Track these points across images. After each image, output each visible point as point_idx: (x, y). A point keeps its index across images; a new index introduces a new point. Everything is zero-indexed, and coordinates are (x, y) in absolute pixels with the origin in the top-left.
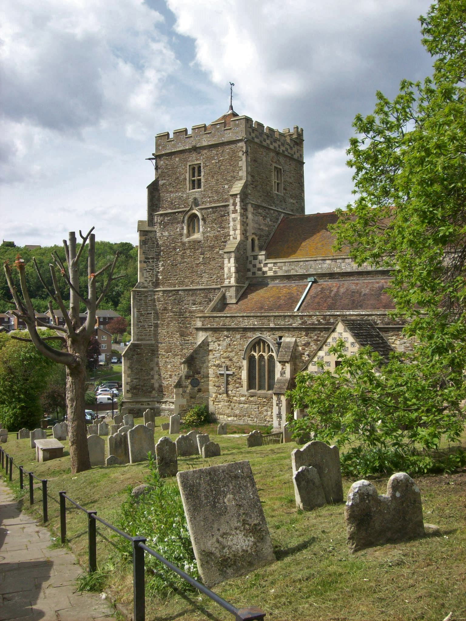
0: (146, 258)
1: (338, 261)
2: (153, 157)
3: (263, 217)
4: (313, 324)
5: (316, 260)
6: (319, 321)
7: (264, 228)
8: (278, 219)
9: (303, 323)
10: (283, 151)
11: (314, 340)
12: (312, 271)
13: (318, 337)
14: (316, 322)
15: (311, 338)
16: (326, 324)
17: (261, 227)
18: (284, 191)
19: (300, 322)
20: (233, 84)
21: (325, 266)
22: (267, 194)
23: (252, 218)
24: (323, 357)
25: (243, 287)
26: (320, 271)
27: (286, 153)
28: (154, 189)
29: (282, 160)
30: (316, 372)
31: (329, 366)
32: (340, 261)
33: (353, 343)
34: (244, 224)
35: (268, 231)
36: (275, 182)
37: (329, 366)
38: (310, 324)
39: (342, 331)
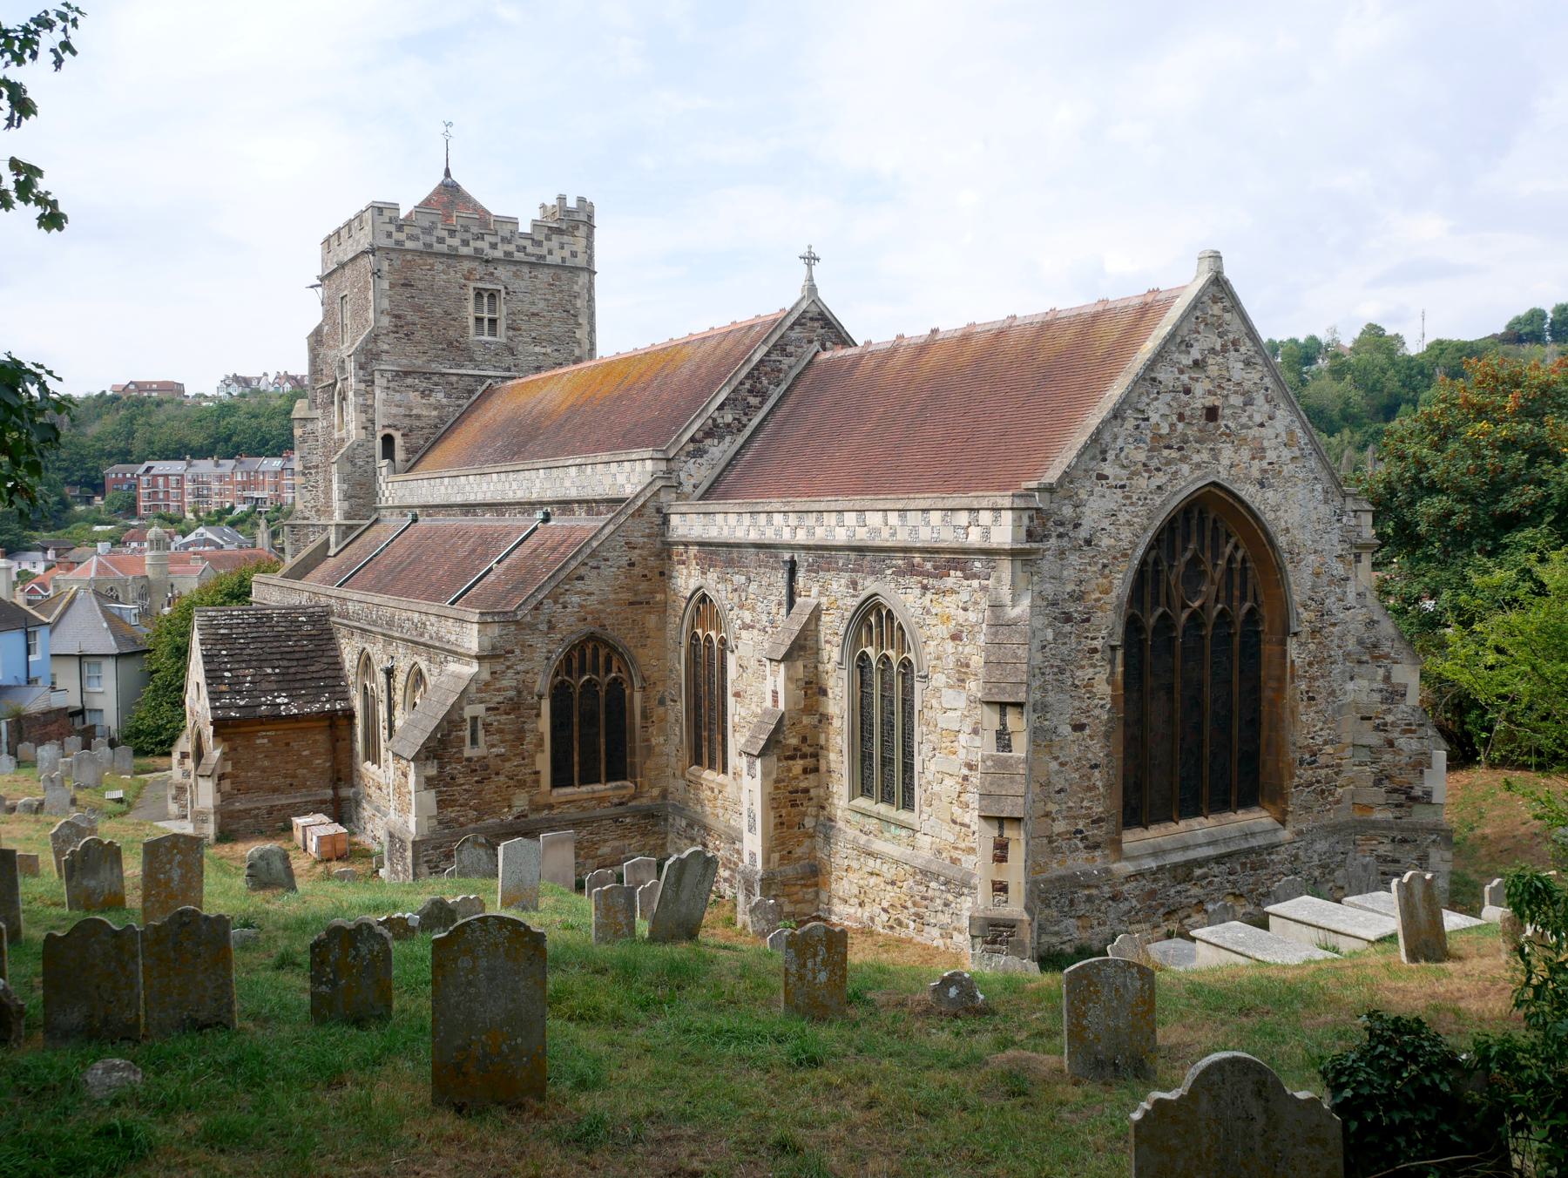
0: (305, 468)
2: (319, 282)
3: (423, 392)
7: (425, 413)
8: (471, 392)
10: (507, 254)
17: (414, 412)
18: (511, 333)
20: (450, 124)
22: (450, 344)
23: (384, 396)
25: (360, 526)
27: (519, 256)
28: (317, 341)
29: (502, 272)
34: (366, 408)
35: (440, 418)
36: (479, 320)
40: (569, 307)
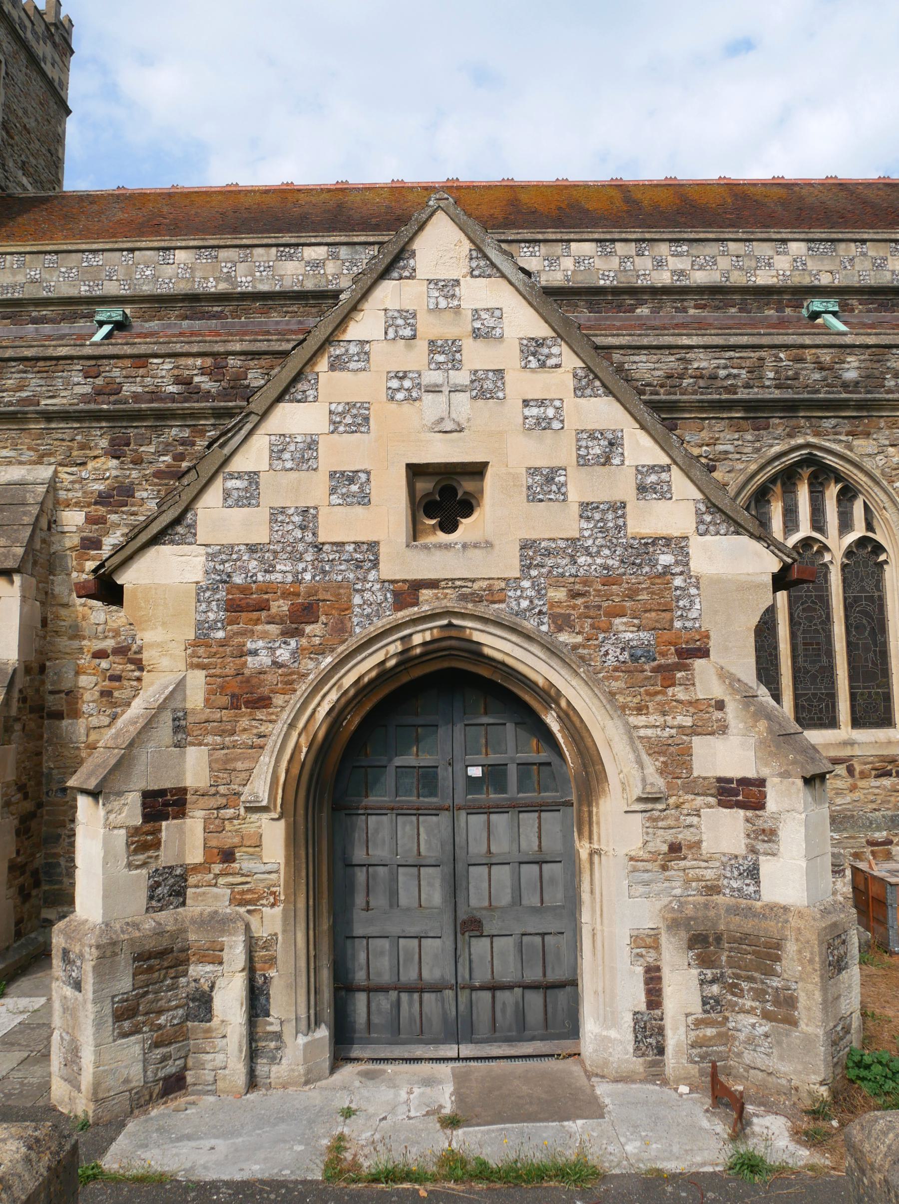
1: (223, 254)
4: (155, 395)
5: (132, 250)
6: (188, 382)
9: (99, 392)
11: (158, 474)
12: (112, 288)
13: (179, 457)
14: (172, 389)
15: (138, 461)
16: (224, 395)
19: (87, 389)
21: (169, 270)
24: (312, 444)
26: (147, 289)
30: (252, 549)
31: (364, 499)
32: (232, 254)
33: (540, 343)
37: (364, 499)
38: (136, 397)
39: (457, 269)
40: (52, 148)
